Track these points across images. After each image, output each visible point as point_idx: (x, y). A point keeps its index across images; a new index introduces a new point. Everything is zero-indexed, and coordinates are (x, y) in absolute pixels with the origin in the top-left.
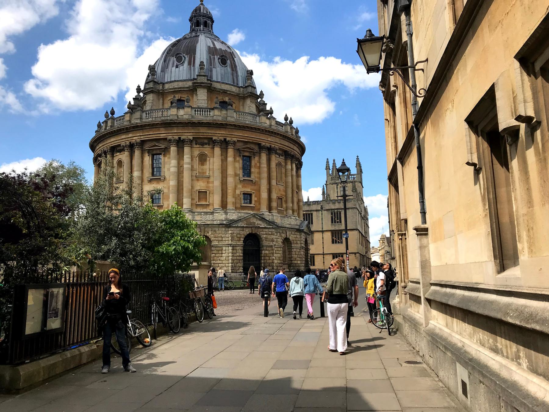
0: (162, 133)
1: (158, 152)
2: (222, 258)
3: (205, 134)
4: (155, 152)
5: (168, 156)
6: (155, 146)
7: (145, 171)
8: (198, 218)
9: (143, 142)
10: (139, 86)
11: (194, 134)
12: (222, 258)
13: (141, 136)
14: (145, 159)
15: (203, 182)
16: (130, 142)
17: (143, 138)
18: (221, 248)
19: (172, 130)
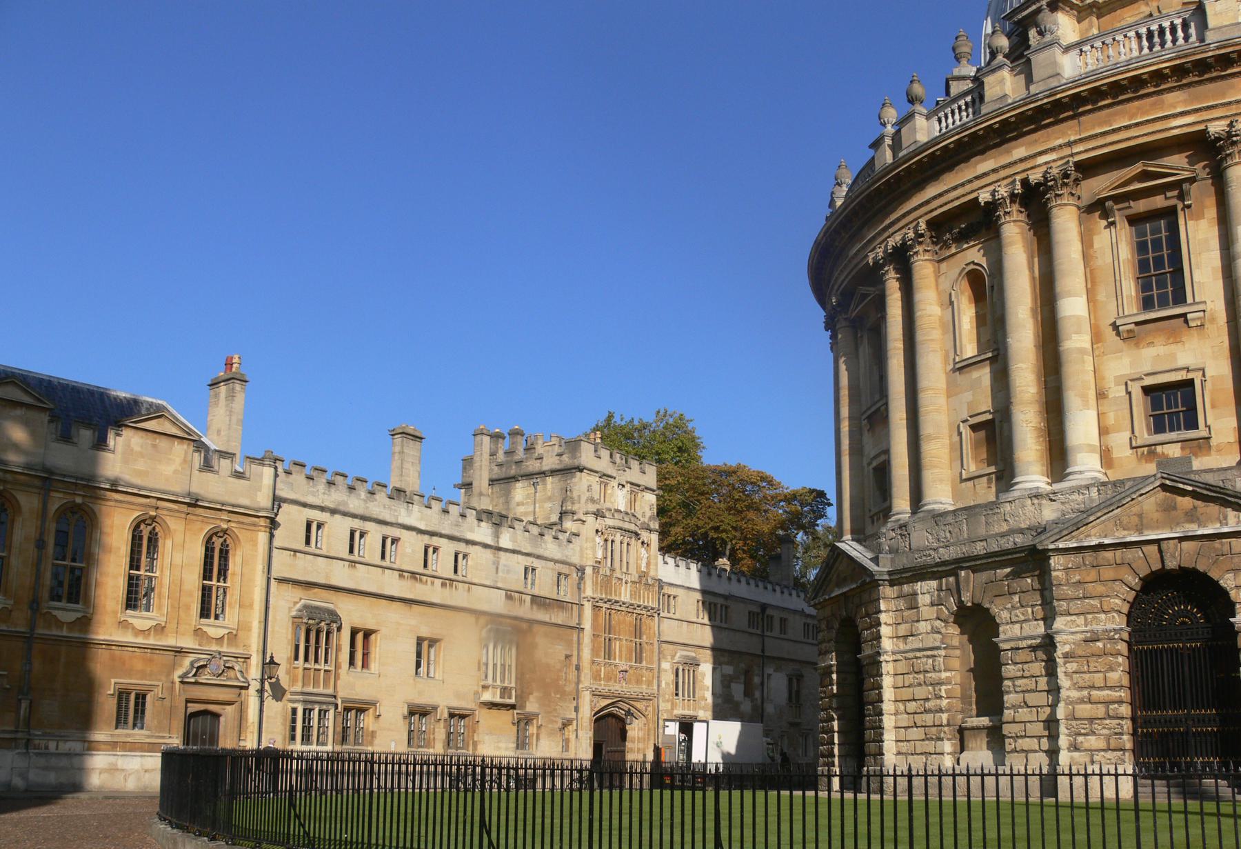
1: (1159, 202)
4: (1141, 206)
13: (1069, 144)
14: (1096, 245)
16: (1025, 182)
19: (1223, 95)
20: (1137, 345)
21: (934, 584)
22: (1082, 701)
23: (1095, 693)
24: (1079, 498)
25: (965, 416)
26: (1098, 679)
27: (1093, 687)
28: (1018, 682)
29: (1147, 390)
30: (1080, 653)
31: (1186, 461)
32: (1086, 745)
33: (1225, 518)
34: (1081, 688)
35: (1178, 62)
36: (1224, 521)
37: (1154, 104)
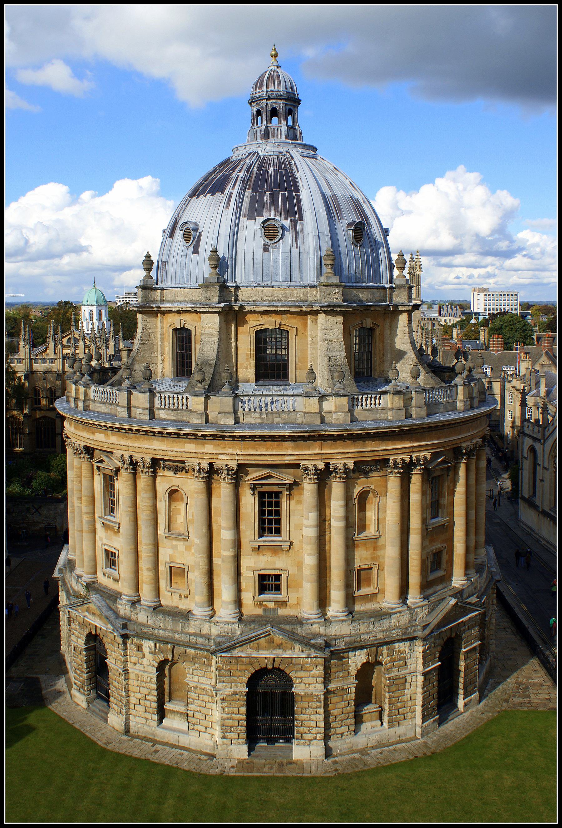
0: (288, 453)
1: (275, 489)
2: (405, 698)
3: (376, 453)
5: (296, 498)
6: (270, 477)
7: (243, 527)
8: (362, 628)
9: (242, 468)
10: (148, 256)
11: (356, 455)
12: (405, 698)
15: (367, 549)
16: (211, 464)
17: (242, 460)
18: (403, 680)
20: (258, 554)
21: (152, 644)
22: (228, 719)
23: (233, 715)
24: (230, 627)
25: (168, 560)
26: (236, 710)
27: (234, 713)
28: (195, 701)
29: (260, 575)
30: (228, 699)
31: (275, 610)
32: (229, 737)
33: (294, 649)
34: (228, 714)
35: (293, 434)
36: (293, 649)
37: (278, 445)
